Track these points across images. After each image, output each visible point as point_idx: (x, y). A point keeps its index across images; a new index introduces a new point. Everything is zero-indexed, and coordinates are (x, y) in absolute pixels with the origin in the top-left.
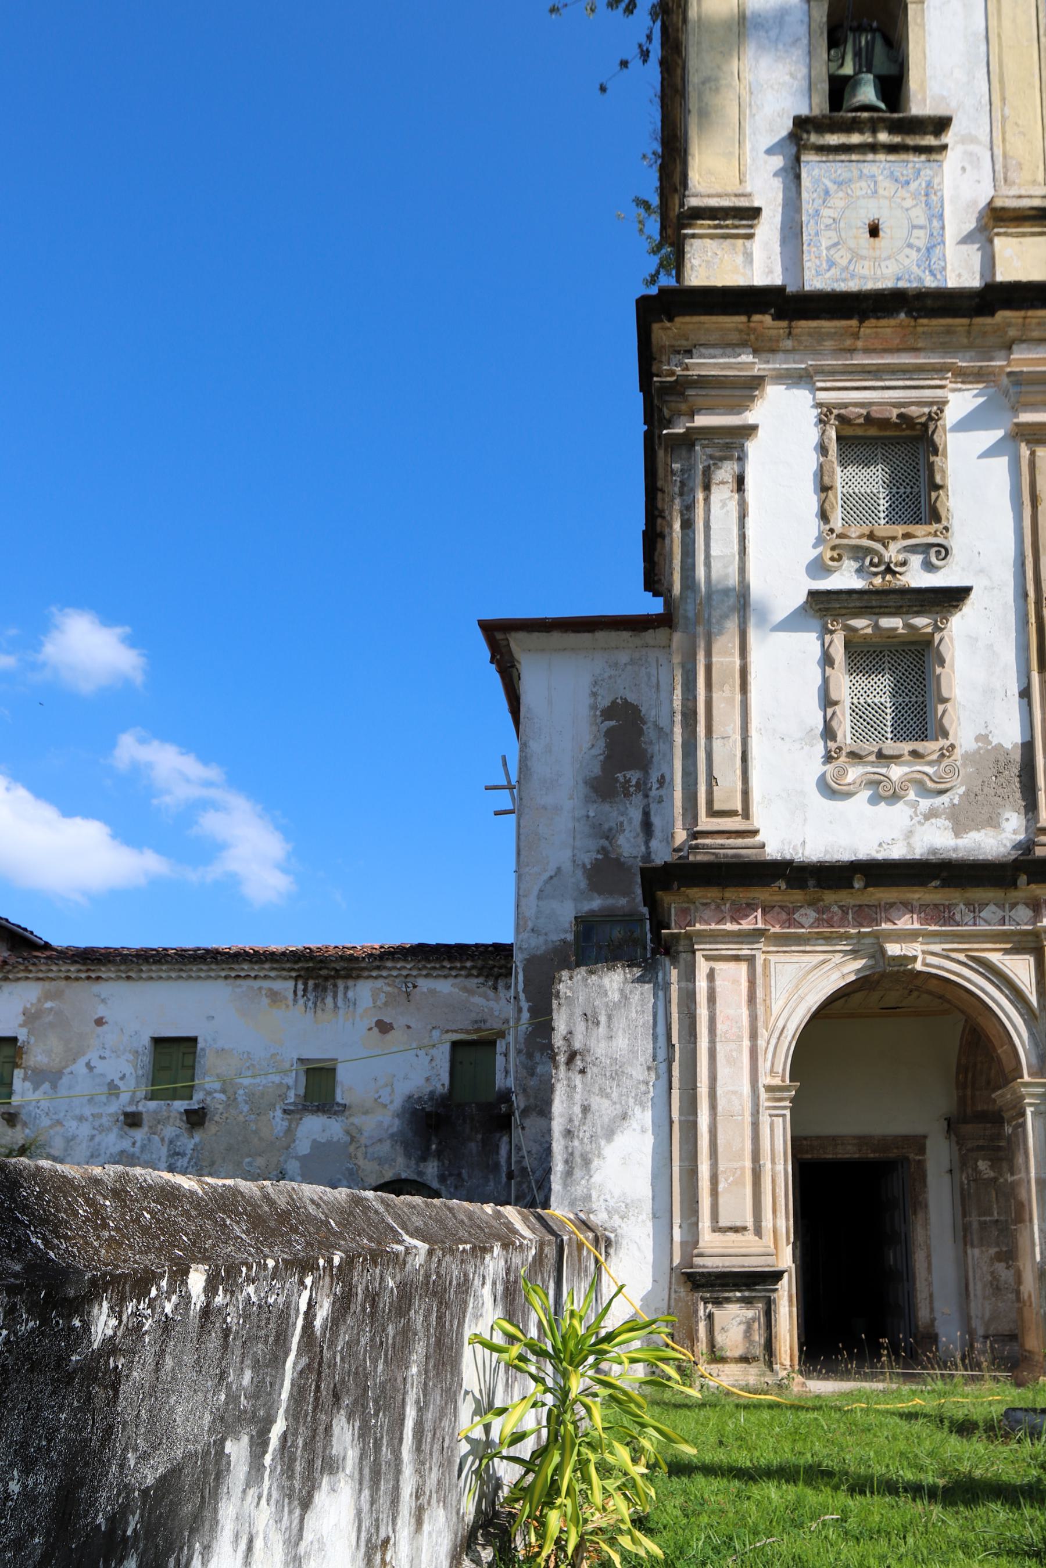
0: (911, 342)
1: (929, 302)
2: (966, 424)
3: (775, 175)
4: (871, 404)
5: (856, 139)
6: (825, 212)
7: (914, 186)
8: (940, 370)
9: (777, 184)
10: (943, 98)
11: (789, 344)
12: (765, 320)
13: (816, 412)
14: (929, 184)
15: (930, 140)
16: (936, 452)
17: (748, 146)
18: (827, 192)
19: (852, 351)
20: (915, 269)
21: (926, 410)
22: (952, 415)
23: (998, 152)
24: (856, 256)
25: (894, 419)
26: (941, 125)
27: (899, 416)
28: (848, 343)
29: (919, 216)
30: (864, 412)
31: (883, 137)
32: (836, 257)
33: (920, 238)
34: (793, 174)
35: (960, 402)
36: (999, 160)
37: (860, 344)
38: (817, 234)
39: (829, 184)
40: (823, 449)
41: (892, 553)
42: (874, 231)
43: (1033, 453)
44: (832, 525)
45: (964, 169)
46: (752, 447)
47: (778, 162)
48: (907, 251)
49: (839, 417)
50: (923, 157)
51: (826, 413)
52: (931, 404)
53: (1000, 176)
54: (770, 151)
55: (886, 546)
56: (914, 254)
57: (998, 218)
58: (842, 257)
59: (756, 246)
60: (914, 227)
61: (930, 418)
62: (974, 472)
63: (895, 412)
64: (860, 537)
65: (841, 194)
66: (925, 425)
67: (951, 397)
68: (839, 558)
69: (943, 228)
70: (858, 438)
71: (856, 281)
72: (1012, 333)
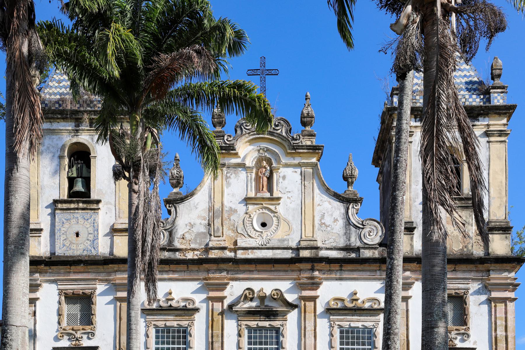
0: (87, 270)
1: (89, 262)
2: (102, 294)
3: (48, 215)
4: (74, 289)
5: (72, 206)
6: (62, 229)
7: (89, 221)
8: (95, 280)
9: (49, 218)
10: (101, 190)
11: (50, 271)
12: (42, 266)
13: (58, 291)
14: (94, 220)
15: (94, 206)
16: (93, 304)
17: (40, 206)
18: (63, 223)
19: (69, 272)
20: (89, 247)
21: (90, 291)
22: (98, 292)
23: (117, 208)
24: (71, 243)
25: (81, 293)
26: (98, 202)
27: (83, 293)
28: (68, 270)
29: (91, 230)
30: (72, 291)
31: (81, 205)
32: (66, 243)
33: (91, 237)
34: (53, 215)
35: (101, 288)
36: (117, 210)
37: (71, 271)
38: (60, 236)
39: (64, 220)
40: (60, 303)
41: (78, 335)
42: (77, 235)
43: (121, 305)
44: (61, 326)
45: (106, 213)
46: (38, 303)
47: (49, 211)
48: (87, 241)
49: (64, 293)
50: (93, 212)
51: (61, 292)
52: (92, 289)
53: (117, 215)
54: (47, 207)
55: (76, 333)
56: (89, 242)
57: (114, 231)
58: (67, 243)
59: (42, 239)
60: (90, 234)
61: (92, 294)
62: (104, 310)
63: (81, 291)
64: (70, 329)
65: (67, 223)
66: (90, 295)
67: (98, 286)
68: (63, 336)
69: (98, 234)
70: (71, 298)
71: (72, 251)
72: (115, 269)
